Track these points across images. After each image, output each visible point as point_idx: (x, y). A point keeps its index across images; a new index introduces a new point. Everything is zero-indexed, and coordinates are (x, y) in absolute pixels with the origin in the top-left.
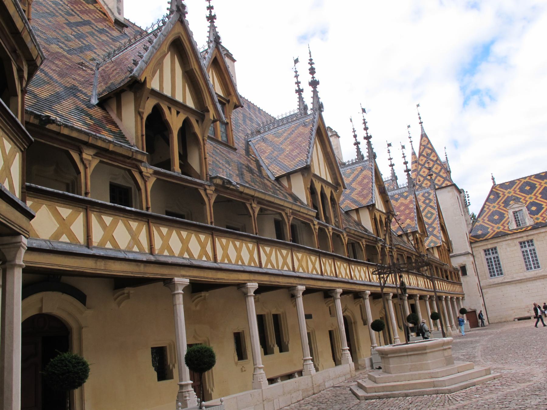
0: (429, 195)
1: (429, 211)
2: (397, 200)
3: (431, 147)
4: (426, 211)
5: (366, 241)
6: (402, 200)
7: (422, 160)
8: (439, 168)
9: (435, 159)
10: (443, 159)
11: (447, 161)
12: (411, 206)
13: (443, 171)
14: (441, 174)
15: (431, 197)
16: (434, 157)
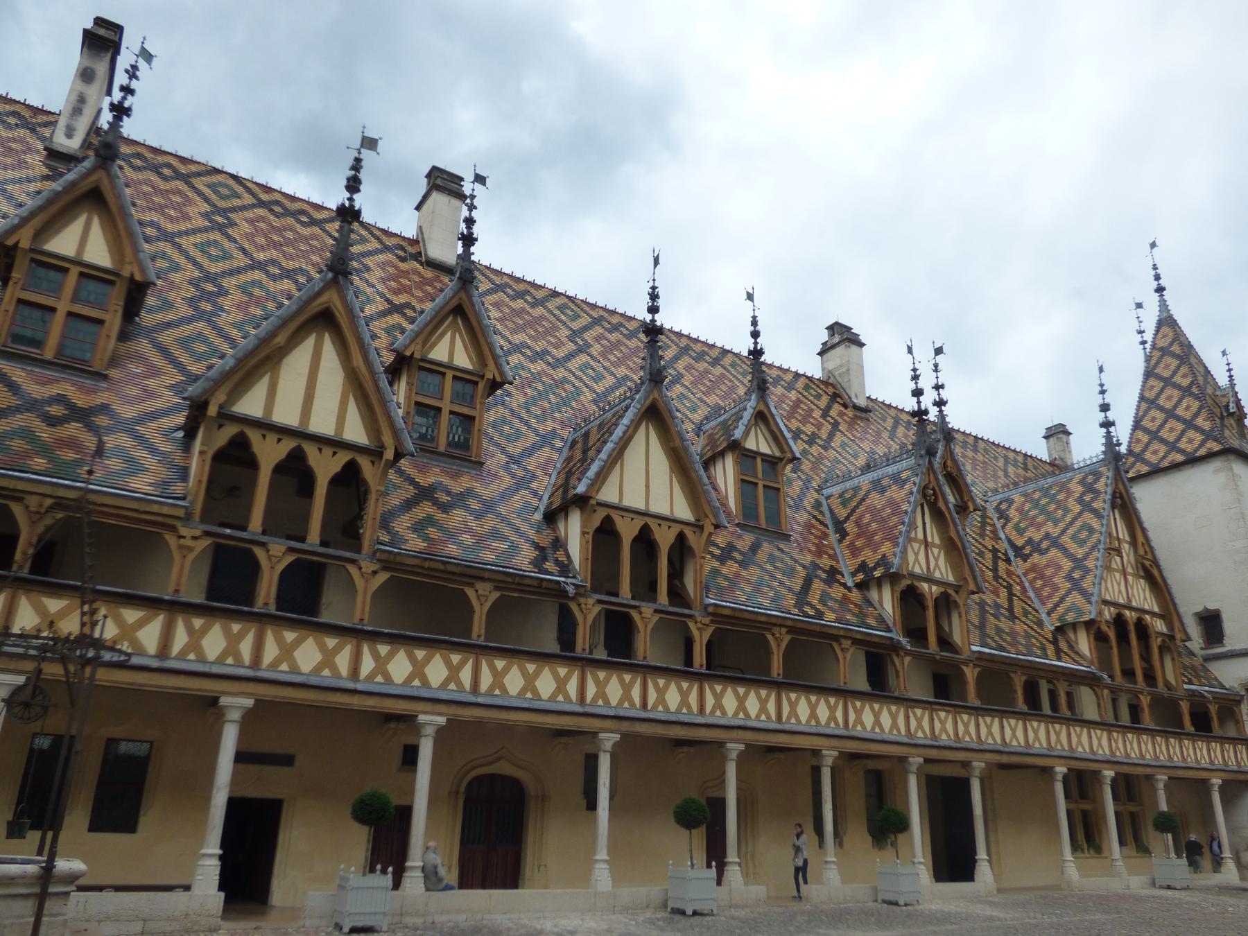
0: (1096, 481)
1: (1085, 524)
2: (882, 491)
3: (1178, 352)
4: (1079, 523)
5: (496, 588)
6: (895, 493)
7: (1152, 387)
8: (1195, 405)
9: (1186, 382)
10: (1223, 380)
11: (1232, 385)
12: (905, 507)
13: (1204, 413)
14: (1199, 421)
15: (1100, 486)
16: (1184, 376)
